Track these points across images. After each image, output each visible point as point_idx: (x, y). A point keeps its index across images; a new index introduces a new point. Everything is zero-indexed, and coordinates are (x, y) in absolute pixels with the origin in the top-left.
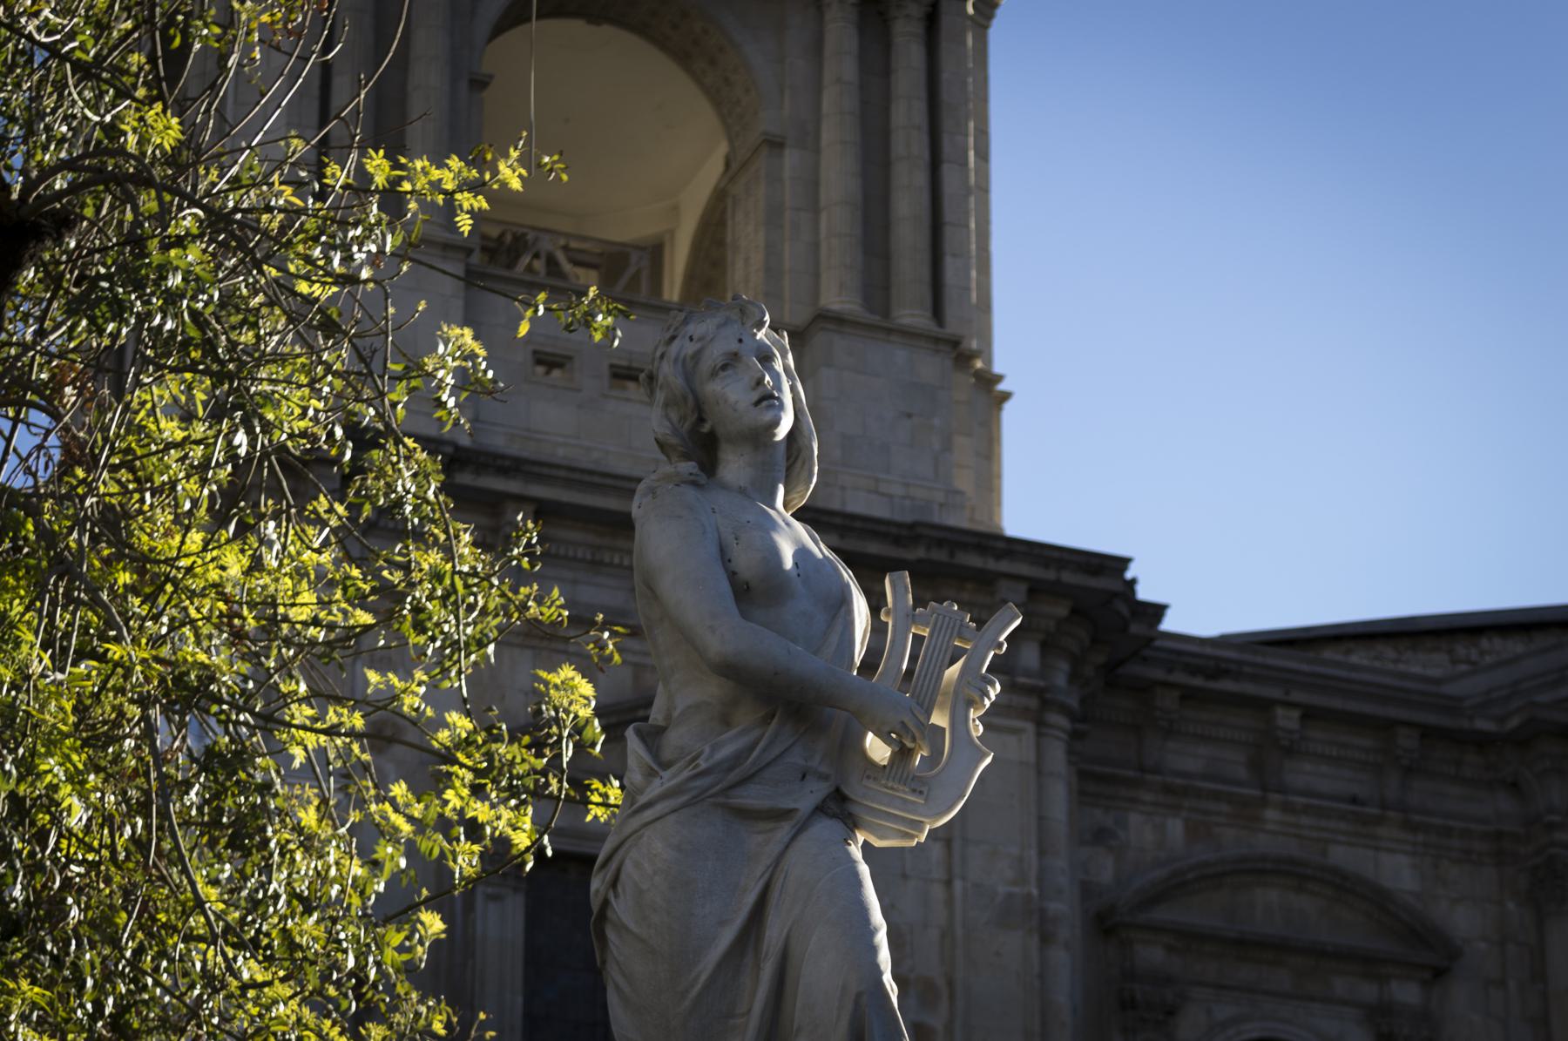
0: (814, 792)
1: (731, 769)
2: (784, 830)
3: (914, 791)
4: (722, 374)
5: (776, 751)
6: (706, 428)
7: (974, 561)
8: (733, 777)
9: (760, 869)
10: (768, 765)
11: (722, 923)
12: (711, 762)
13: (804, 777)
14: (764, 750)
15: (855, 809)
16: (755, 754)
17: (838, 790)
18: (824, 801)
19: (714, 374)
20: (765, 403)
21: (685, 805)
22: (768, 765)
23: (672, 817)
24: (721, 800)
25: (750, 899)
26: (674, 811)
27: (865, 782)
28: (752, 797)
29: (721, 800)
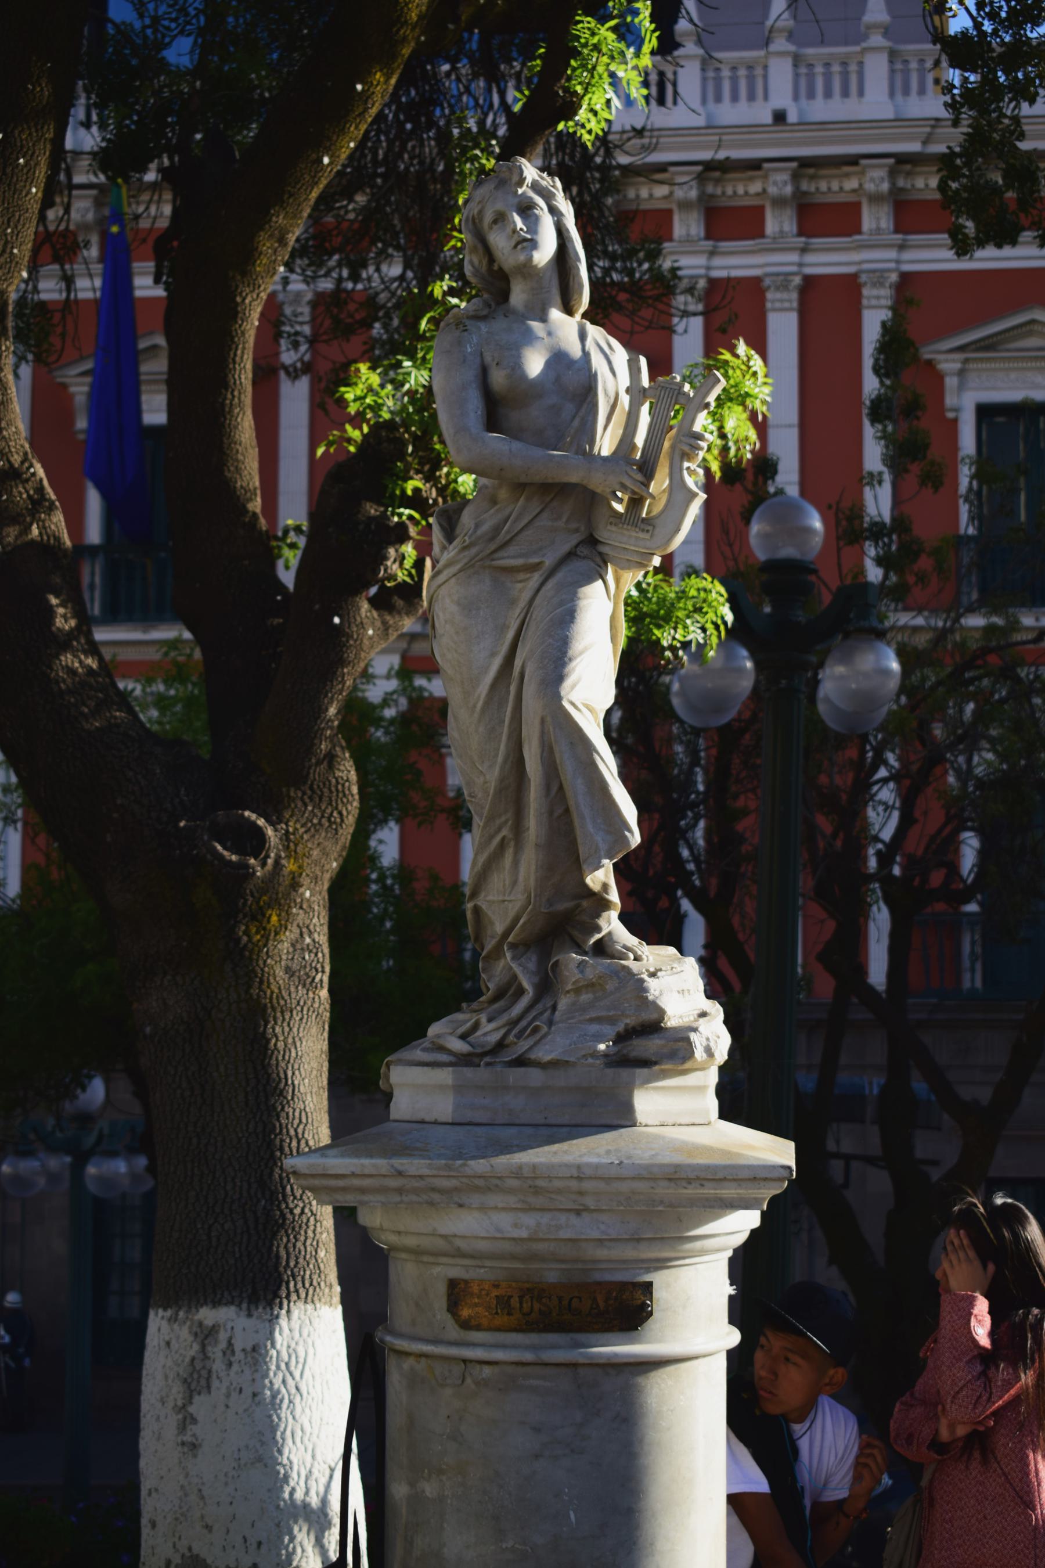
1: (492, 539)
2: (536, 578)
3: (643, 530)
4: (495, 227)
6: (496, 268)
8: (493, 546)
9: (518, 611)
11: (493, 655)
12: (473, 538)
14: (514, 522)
15: (603, 549)
16: (508, 524)
17: (591, 535)
18: (577, 546)
19: (491, 228)
20: (519, 247)
21: (460, 571)
23: (453, 580)
24: (488, 563)
25: (510, 635)
26: (454, 575)
27: (609, 527)
29: (488, 563)
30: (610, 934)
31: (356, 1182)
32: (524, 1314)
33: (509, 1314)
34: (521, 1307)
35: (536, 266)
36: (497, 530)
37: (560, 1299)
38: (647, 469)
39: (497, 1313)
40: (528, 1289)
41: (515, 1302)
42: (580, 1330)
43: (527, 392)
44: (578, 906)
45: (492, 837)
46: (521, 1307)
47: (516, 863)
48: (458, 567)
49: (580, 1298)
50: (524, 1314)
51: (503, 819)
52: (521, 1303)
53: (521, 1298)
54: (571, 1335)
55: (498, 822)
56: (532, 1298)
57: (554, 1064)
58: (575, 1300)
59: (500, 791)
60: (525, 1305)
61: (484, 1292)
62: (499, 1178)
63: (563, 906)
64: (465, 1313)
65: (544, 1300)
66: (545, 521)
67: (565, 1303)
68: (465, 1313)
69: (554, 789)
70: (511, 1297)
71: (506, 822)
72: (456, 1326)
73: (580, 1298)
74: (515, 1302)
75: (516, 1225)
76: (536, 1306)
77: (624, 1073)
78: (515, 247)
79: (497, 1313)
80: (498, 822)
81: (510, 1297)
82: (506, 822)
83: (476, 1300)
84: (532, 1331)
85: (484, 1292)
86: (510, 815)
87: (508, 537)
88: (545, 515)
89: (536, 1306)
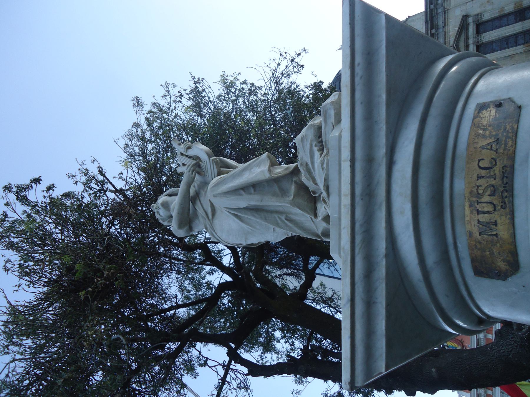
7: (429, 13)
8: (207, 219)
11: (234, 220)
19: (161, 216)
21: (214, 231)
32: (495, 210)
33: (495, 224)
34: (488, 212)
36: (203, 217)
37: (479, 177)
39: (496, 235)
40: (471, 206)
41: (484, 218)
42: (512, 158)
44: (296, 182)
45: (287, 225)
46: (488, 212)
47: (296, 214)
49: (479, 161)
50: (495, 210)
51: (278, 219)
52: (484, 213)
53: (478, 212)
54: (517, 166)
55: (279, 221)
56: (478, 203)
58: (481, 165)
59: (266, 220)
60: (486, 209)
61: (479, 246)
63: (293, 189)
64: (502, 265)
65: (481, 192)
67: (483, 173)
68: (502, 265)
69: (242, 192)
70: (479, 222)
71: (280, 218)
72: (518, 275)
73: (479, 161)
74: (484, 218)
76: (486, 198)
79: (496, 235)
80: (279, 221)
81: (479, 222)
82: (280, 218)
83: (487, 253)
84: (512, 202)
85: (479, 246)
86: (276, 216)
87: (204, 213)
89: (486, 198)
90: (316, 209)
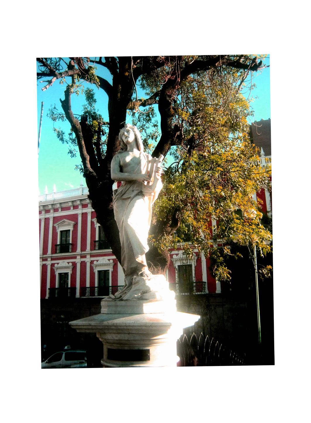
0: (136, 192)
1: (121, 194)
2: (129, 200)
5: (127, 188)
8: (121, 195)
10: (126, 191)
13: (133, 191)
14: (125, 189)
15: (143, 193)
17: (141, 191)
21: (116, 200)
22: (126, 191)
23: (115, 203)
24: (121, 198)
26: (115, 201)
28: (125, 197)
30: (144, 272)
31: (83, 327)
35: (129, 142)
36: (122, 191)
38: (150, 176)
43: (127, 165)
48: (116, 199)
57: (127, 300)
62: (110, 326)
66: (131, 189)
75: (116, 337)
77: (141, 301)
78: (125, 138)
88: (131, 187)
90: (129, 275)
